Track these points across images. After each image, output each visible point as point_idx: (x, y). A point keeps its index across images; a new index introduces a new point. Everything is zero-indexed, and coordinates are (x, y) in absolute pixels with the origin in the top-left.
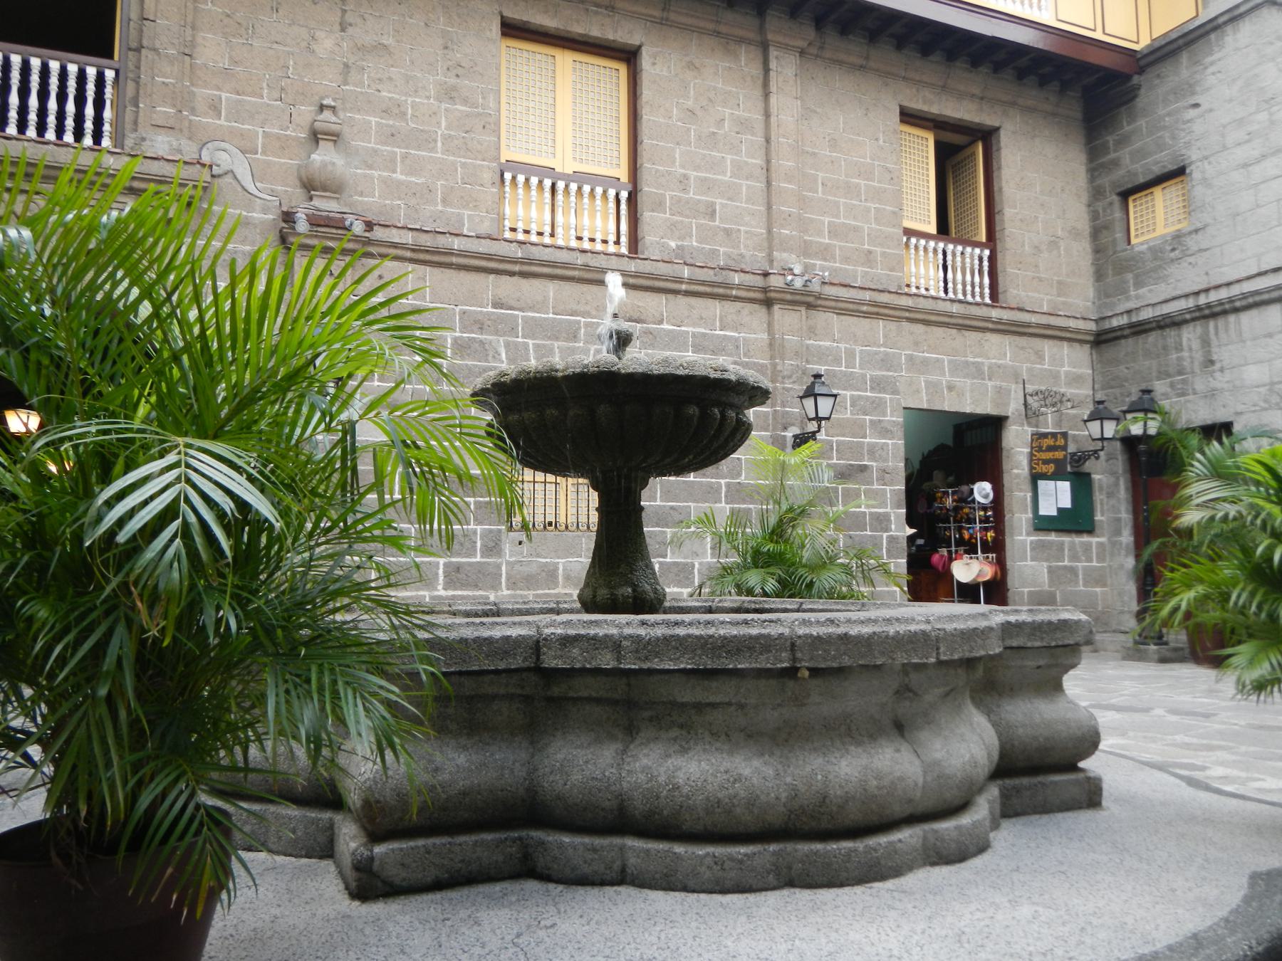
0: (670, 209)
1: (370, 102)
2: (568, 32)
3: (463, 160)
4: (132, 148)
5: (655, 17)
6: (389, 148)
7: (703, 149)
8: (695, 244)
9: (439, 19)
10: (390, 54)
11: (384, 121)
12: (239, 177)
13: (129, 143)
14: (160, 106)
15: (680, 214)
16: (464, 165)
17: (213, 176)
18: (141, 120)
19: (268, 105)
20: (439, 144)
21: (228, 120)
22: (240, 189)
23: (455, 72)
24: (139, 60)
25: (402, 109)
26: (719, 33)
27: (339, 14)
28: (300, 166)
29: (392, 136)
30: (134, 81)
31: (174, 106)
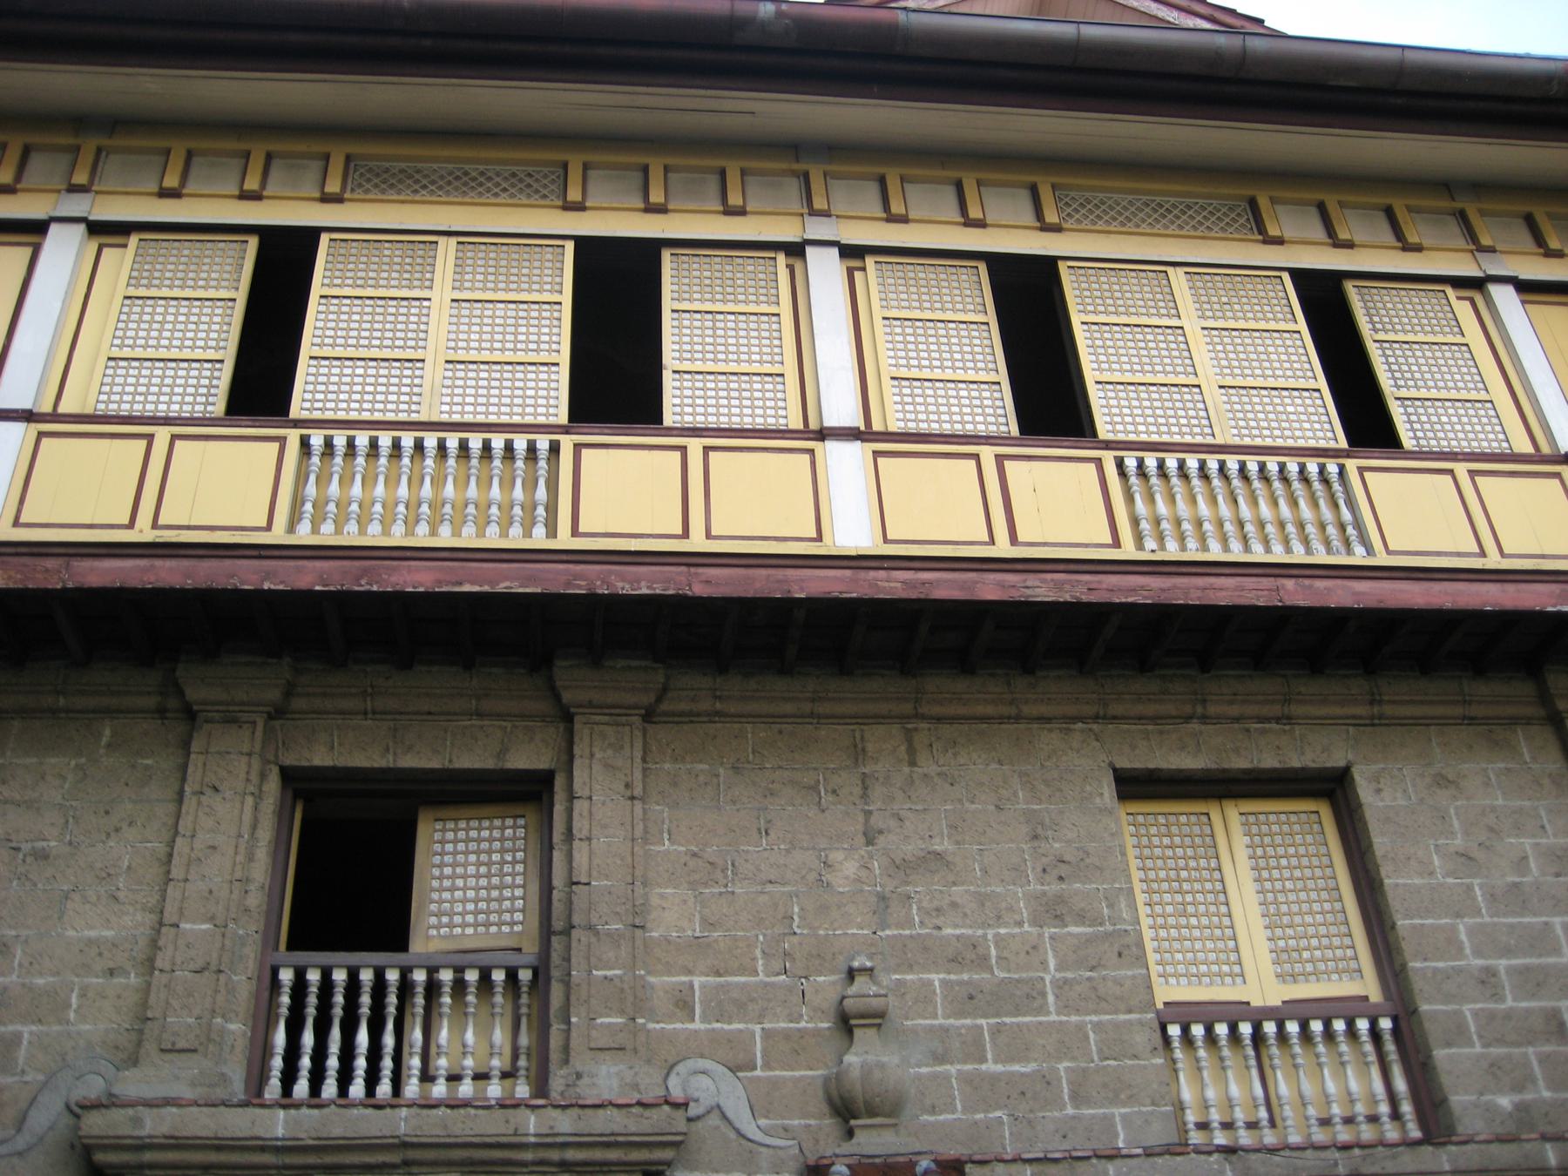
0: (1480, 1037)
1: (926, 949)
2: (1224, 770)
3: (1094, 1018)
4: (562, 1094)
5: (1361, 718)
6: (968, 1021)
7: (1505, 915)
8: (1546, 1094)
9: (1015, 794)
10: (948, 864)
11: (953, 977)
12: (730, 1114)
13: (557, 1084)
14: (601, 1016)
15: (1501, 1041)
16: (1098, 1027)
17: (690, 1120)
18: (574, 1043)
19: (766, 984)
20: (1051, 998)
21: (704, 1019)
22: (733, 1135)
23: (1055, 873)
24: (568, 948)
25: (980, 950)
26: (1472, 718)
27: (861, 818)
28: (826, 1080)
29: (968, 1000)
30: (562, 981)
31: (622, 1012)
